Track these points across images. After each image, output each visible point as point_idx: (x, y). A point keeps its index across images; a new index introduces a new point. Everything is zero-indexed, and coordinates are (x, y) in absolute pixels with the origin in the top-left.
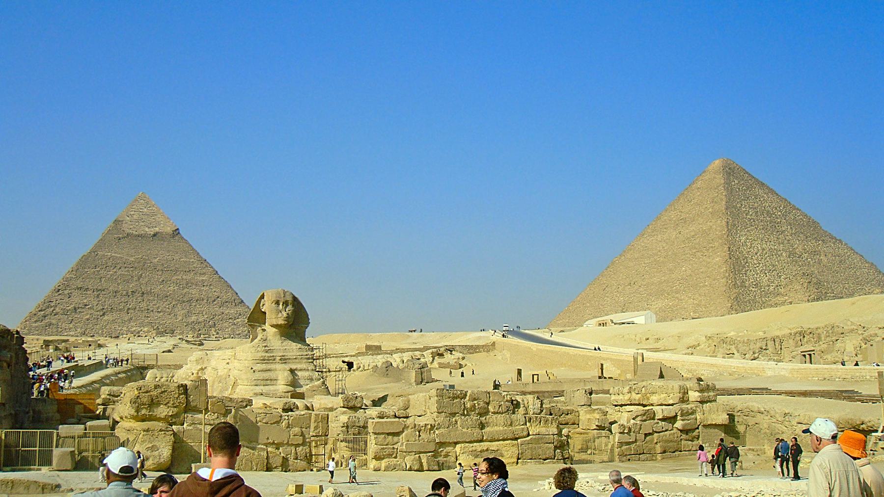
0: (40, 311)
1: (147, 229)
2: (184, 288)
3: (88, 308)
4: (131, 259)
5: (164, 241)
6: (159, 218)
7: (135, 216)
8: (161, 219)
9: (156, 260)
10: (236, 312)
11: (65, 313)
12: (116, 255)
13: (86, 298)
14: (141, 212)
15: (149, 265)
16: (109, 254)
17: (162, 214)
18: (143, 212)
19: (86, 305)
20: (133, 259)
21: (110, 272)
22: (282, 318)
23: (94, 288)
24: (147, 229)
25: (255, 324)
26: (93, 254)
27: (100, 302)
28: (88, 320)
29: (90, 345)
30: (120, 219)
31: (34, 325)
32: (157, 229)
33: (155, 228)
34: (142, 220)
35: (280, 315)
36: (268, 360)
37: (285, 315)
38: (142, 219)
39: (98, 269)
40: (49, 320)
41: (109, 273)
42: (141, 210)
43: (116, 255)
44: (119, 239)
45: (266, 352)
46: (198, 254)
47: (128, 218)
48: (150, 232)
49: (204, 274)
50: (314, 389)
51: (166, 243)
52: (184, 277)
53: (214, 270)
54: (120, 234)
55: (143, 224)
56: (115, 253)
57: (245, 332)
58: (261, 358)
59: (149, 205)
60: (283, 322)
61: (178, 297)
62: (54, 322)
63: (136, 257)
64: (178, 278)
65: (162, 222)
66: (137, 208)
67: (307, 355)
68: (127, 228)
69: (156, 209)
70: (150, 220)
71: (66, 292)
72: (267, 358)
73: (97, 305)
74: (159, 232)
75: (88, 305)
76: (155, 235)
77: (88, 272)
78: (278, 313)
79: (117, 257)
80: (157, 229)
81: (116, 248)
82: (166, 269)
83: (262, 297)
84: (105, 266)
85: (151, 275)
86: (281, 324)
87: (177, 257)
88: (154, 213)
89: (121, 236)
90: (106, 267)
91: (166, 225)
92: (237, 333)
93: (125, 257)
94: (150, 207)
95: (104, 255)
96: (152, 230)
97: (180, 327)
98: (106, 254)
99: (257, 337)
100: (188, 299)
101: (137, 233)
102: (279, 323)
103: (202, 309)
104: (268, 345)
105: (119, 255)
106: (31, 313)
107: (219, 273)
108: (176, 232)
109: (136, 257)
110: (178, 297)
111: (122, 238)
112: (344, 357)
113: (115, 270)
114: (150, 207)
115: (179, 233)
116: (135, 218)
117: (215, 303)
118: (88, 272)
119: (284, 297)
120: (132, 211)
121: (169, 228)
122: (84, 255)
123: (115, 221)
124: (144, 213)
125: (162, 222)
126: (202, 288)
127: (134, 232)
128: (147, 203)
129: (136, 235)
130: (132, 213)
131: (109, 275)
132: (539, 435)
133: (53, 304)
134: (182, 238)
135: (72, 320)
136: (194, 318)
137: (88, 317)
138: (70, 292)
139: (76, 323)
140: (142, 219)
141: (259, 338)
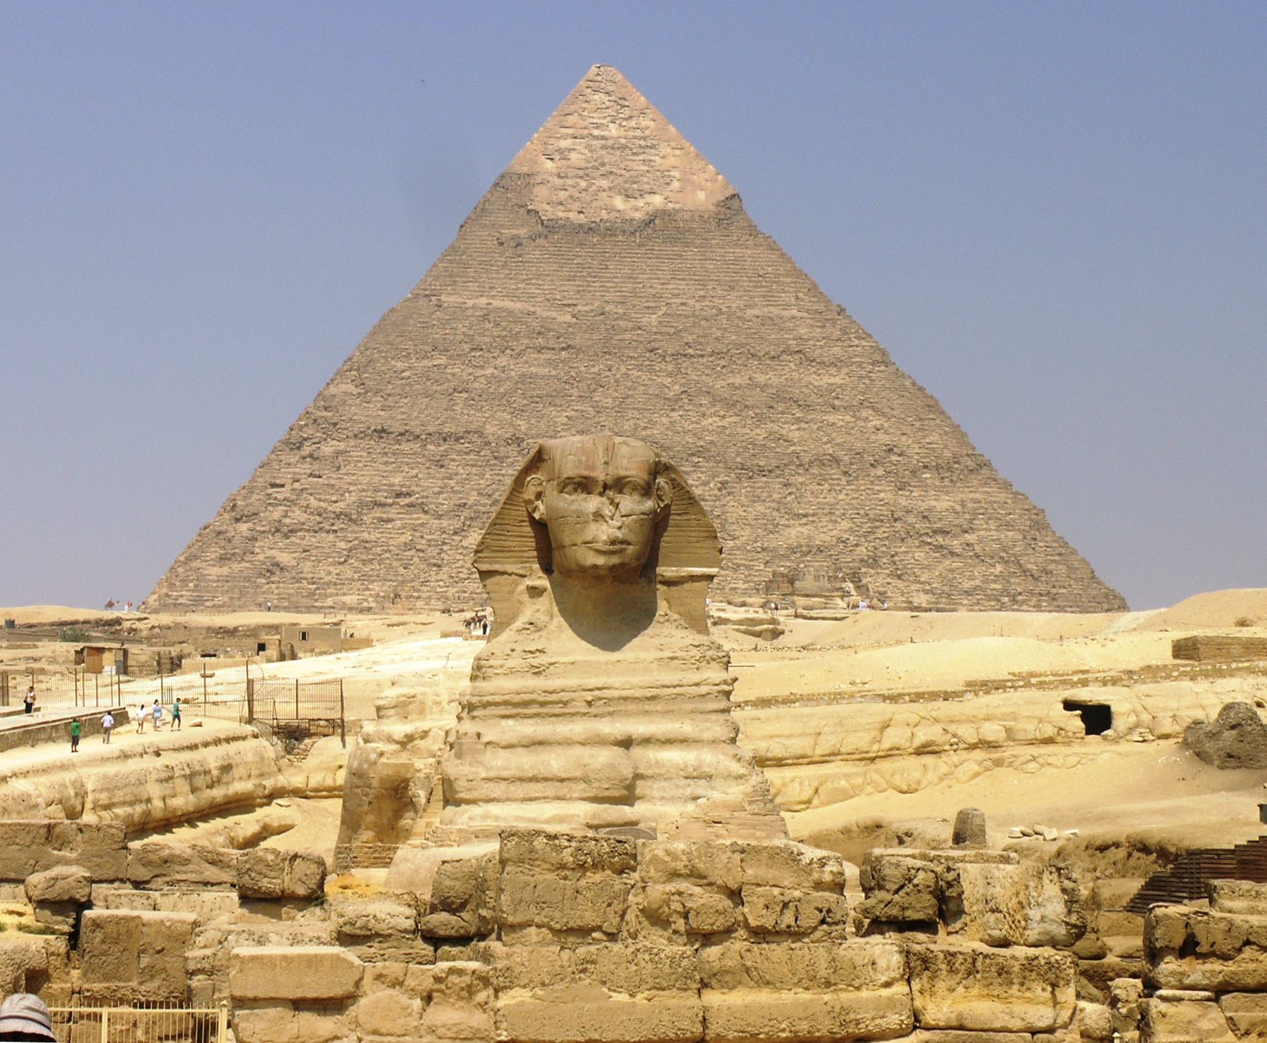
0: (237, 520)
1: (619, 202)
2: (760, 419)
3: (411, 505)
4: (560, 319)
5: (687, 245)
6: (663, 157)
7: (573, 156)
8: (672, 161)
9: (654, 316)
10: (958, 508)
11: (331, 521)
13: (398, 470)
14: (596, 138)
15: (628, 336)
17: (673, 144)
18: (603, 138)
19: (399, 495)
20: (568, 318)
21: (482, 368)
22: (599, 546)
23: (431, 429)
24: (619, 202)
25: (510, 568)
26: (423, 302)
27: (452, 483)
28: (408, 546)
29: (262, 647)
30: (525, 170)
31: (214, 571)
32: (657, 200)
33: (648, 198)
34: (603, 170)
36: (543, 704)
38: (603, 165)
39: (442, 361)
40: (270, 553)
41: (480, 372)
42: (596, 132)
43: (508, 304)
44: (519, 244)
45: (538, 672)
46: (815, 286)
47: (549, 164)
48: (635, 209)
49: (836, 364)
50: (715, 815)
51: (691, 252)
52: (761, 378)
53: (876, 348)
54: (522, 226)
55: (604, 183)
56: (513, 297)
57: (995, 582)
58: (517, 699)
59: (627, 112)
60: (601, 561)
61: (738, 454)
62: (285, 558)
63: (579, 308)
64: (737, 380)
65: (676, 173)
66: (581, 123)
67: (697, 685)
68: (541, 199)
69: (652, 124)
70: (631, 165)
71: (327, 449)
72: (541, 699)
73: (439, 493)
74: (664, 212)
75: (408, 494)
76: (649, 223)
77: (407, 374)
78: (587, 522)
79: (511, 312)
81: (507, 276)
82: (691, 351)
84: (466, 347)
85: (635, 373)
86: (595, 567)
87: (734, 301)
88: (644, 138)
89: (522, 232)
90: (472, 350)
91: (687, 181)
92: (967, 585)
93: (539, 310)
94: (631, 117)
95: (462, 308)
96: (640, 203)
97: (747, 567)
98: (470, 303)
99: (514, 617)
100: (774, 463)
101: (582, 219)
103: (830, 499)
104: (550, 648)
105: (518, 305)
106: (205, 528)
107: (893, 358)
108: (730, 208)
109: (579, 308)
110: (738, 454)
111: (532, 238)
112: (1074, 685)
113: (503, 361)
114: (631, 117)
115: (740, 211)
116: (578, 164)
117: (880, 472)
118: (407, 374)
119: (606, 463)
120: (565, 137)
121: (701, 195)
122: (393, 310)
123: (502, 176)
124: (610, 143)
125: (676, 173)
126: (831, 418)
127: (571, 215)
128: (621, 103)
129: (581, 226)
130: (564, 144)
131: (482, 380)
132: (961, 1028)
133: (281, 494)
134: (753, 231)
135: (350, 550)
136: (795, 533)
137: (406, 537)
138: (342, 446)
139: (364, 562)
140: (603, 165)
141: (519, 624)
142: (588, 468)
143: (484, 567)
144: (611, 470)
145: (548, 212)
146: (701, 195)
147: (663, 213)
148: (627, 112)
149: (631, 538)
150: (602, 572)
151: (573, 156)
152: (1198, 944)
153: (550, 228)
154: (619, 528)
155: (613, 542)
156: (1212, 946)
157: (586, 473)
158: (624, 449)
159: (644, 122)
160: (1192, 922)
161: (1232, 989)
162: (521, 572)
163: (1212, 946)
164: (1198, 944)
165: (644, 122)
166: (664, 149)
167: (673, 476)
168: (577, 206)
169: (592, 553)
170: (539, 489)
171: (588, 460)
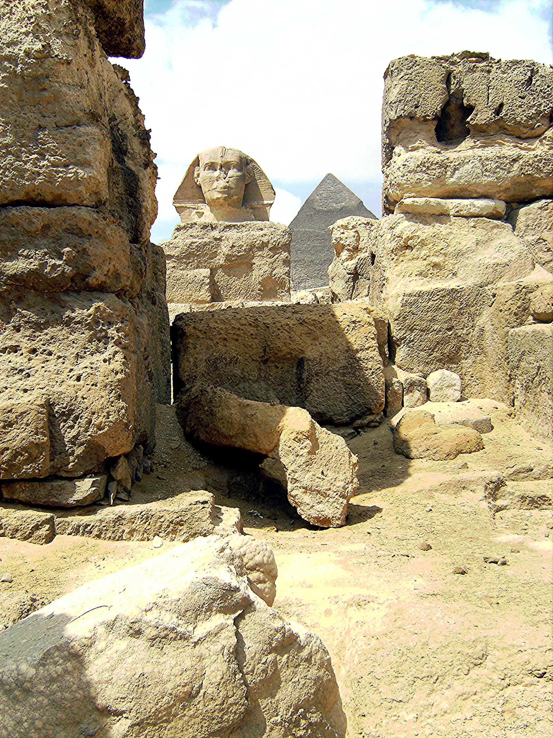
1: (334, 205)
7: (323, 195)
8: (346, 195)
12: (309, 230)
16: (303, 230)
22: (218, 190)
24: (334, 205)
25: (188, 205)
32: (343, 204)
35: (215, 184)
37: (222, 183)
43: (309, 230)
48: (339, 206)
55: (331, 201)
56: (310, 228)
59: (335, 184)
60: (220, 196)
68: (316, 205)
80: (343, 204)
83: (196, 162)
86: (218, 198)
102: (215, 198)
113: (308, 243)
121: (354, 202)
130: (321, 192)
142: (214, 159)
143: (177, 205)
144: (224, 159)
145: (318, 208)
146: (354, 202)
147: (344, 207)
148: (335, 184)
149: (233, 186)
150: (221, 201)
151: (323, 195)
152: (470, 109)
153: (319, 211)
154: (227, 182)
155: (224, 188)
156: (498, 111)
157: (213, 161)
158: (230, 151)
159: (339, 186)
160: (456, 69)
161: (536, 192)
162: (194, 207)
163: (498, 111)
164: (470, 109)
165: (339, 186)
166: (344, 192)
167: (253, 164)
168: (325, 206)
169: (217, 193)
170: (198, 172)
171: (214, 156)
